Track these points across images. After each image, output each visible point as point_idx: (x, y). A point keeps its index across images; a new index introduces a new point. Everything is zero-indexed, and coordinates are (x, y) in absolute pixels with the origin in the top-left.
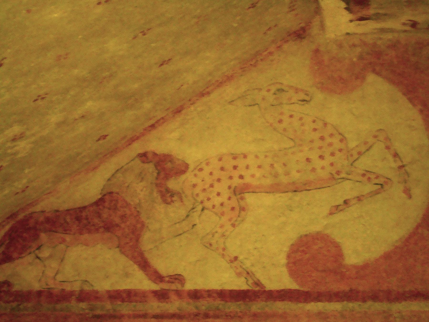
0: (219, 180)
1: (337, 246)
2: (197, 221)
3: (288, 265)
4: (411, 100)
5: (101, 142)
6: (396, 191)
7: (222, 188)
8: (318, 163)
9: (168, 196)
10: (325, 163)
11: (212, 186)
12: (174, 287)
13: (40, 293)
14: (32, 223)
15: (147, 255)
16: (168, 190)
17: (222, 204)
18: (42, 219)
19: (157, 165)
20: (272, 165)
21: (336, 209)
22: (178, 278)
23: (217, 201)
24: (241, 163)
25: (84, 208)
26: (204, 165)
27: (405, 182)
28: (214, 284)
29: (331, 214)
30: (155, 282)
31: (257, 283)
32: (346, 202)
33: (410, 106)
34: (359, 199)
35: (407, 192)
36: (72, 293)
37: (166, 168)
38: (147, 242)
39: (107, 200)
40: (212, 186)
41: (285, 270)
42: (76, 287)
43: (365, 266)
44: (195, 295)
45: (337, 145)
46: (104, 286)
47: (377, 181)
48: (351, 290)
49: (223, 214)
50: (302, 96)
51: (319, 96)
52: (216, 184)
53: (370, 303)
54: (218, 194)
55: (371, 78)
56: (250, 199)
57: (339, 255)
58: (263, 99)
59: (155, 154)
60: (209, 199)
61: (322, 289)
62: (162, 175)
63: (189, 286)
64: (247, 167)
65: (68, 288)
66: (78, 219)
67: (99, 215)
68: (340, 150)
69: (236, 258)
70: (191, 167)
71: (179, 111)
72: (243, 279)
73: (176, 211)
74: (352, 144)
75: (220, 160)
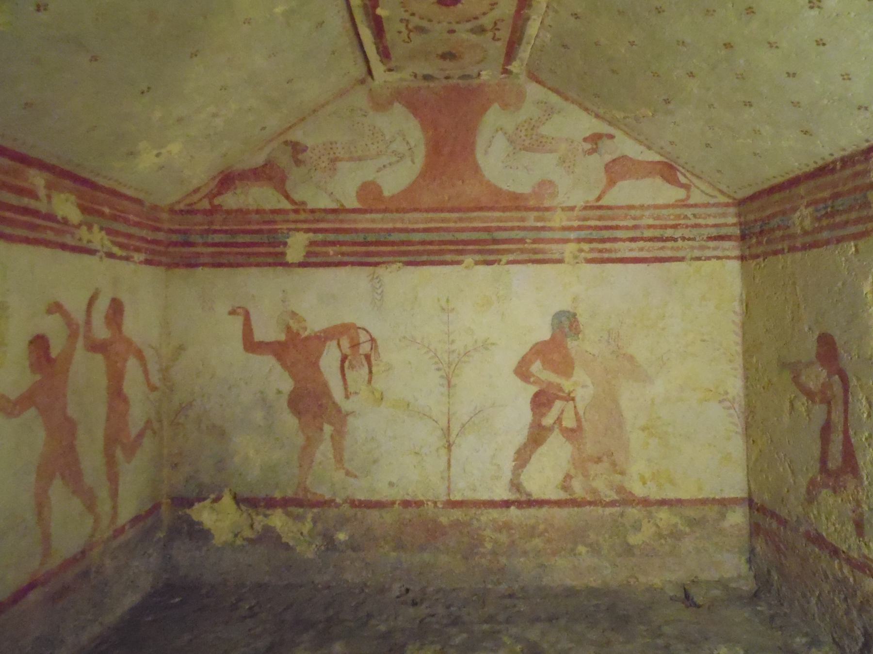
9: (298, 163)
10: (374, 147)
23: (323, 165)
24: (334, 146)
28: (322, 206)
31: (342, 205)
32: (384, 166)
34: (390, 164)
35: (413, 162)
37: (297, 149)
38: (289, 186)
39: (269, 164)
42: (255, 207)
43: (393, 196)
44: (313, 211)
46: (268, 207)
56: (339, 165)
57: (381, 192)
61: (374, 208)
63: (310, 206)
65: (251, 208)
66: (255, 174)
74: (387, 138)
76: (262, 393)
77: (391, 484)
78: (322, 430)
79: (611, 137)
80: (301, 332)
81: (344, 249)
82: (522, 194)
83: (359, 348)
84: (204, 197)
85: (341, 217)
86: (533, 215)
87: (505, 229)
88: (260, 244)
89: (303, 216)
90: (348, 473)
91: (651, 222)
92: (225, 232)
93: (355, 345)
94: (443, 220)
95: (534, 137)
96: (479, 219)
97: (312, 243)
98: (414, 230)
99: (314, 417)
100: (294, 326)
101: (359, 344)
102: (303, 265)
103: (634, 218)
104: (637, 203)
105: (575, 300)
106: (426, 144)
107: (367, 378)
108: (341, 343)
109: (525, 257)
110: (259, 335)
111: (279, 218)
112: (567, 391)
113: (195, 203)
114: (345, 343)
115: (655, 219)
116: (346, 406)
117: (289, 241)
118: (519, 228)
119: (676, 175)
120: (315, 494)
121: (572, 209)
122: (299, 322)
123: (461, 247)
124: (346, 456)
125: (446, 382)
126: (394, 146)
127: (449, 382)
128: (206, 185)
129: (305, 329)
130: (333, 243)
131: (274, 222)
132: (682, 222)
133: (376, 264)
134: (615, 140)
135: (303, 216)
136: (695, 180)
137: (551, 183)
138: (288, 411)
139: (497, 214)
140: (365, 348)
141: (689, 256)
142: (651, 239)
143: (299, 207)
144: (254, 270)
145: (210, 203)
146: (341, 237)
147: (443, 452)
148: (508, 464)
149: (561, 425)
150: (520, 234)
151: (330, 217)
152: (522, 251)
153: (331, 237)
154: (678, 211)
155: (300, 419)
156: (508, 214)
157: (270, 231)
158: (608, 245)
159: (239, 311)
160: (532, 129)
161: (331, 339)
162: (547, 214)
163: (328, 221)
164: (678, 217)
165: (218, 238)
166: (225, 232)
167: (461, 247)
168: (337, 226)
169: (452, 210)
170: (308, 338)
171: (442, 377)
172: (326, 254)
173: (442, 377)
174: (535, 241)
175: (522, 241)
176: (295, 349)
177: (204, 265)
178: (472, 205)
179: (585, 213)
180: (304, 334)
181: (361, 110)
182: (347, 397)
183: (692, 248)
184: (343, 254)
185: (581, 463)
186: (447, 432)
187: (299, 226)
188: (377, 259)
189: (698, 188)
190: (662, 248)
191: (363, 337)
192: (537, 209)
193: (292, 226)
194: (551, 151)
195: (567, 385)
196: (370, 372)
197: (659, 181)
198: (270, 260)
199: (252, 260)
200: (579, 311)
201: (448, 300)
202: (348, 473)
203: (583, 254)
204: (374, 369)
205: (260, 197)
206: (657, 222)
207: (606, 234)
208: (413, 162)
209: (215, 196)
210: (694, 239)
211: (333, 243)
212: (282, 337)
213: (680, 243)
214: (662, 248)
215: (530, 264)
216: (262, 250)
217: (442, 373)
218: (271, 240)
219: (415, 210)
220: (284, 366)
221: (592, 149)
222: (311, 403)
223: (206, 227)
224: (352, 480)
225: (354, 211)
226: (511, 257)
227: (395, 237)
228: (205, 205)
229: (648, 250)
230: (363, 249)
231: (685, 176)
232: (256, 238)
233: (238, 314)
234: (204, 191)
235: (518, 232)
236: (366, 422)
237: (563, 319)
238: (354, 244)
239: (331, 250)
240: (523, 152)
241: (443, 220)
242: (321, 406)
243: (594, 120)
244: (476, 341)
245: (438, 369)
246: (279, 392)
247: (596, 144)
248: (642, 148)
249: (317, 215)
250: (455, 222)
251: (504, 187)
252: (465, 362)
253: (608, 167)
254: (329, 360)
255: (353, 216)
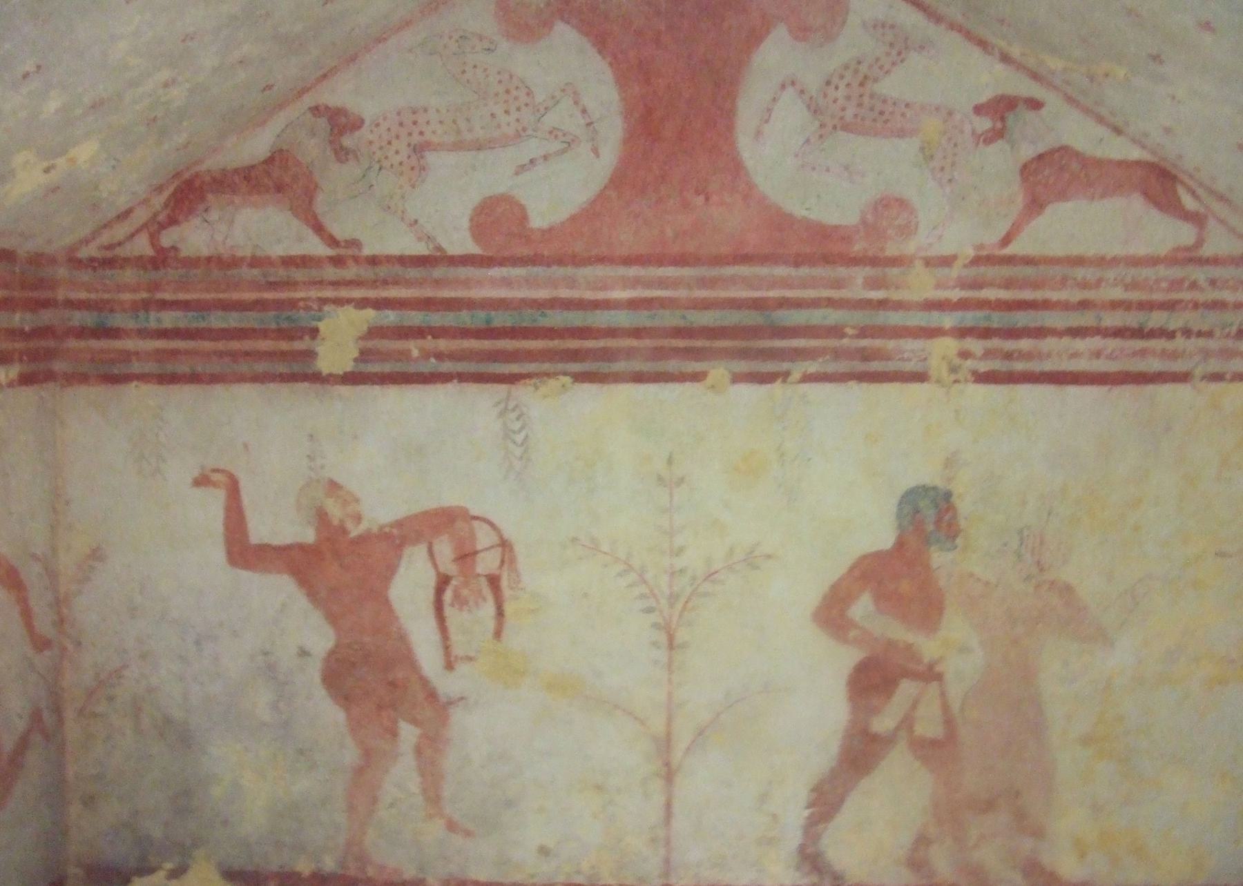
0: (398, 137)
1: (522, 208)
2: (374, 183)
3: (471, 229)
4: (600, 52)
5: (267, 92)
6: (584, 149)
7: (402, 145)
8: (503, 119)
9: (342, 154)
11: (389, 143)
12: (350, 252)
13: (209, 259)
14: (197, 183)
15: (319, 217)
16: (342, 148)
17: (401, 164)
18: (208, 179)
19: (331, 119)
20: (454, 122)
21: (521, 169)
22: (354, 243)
23: (396, 159)
25: (253, 167)
26: (381, 121)
27: (593, 139)
29: (517, 174)
30: (329, 246)
31: (439, 248)
32: (532, 161)
33: (599, 57)
34: (545, 158)
35: (596, 151)
36: (242, 259)
37: (340, 123)
38: (321, 205)
39: (278, 158)
40: (389, 143)
41: (467, 234)
42: (247, 252)
43: (551, 229)
44: (374, 261)
45: (524, 99)
47: (564, 139)
48: (536, 255)
49: (402, 174)
50: (486, 45)
51: (504, 45)
52: (395, 142)
53: (555, 268)
54: (397, 152)
55: (560, 27)
56: (431, 158)
57: (524, 218)
58: (445, 46)
59: (327, 108)
60: (386, 158)
61: (506, 254)
62: (336, 131)
63: (367, 251)
64: (428, 123)
65: (240, 254)
66: (247, 178)
67: (268, 174)
68: (527, 105)
69: (416, 221)
70: (367, 123)
71: (353, 59)
72: (423, 243)
73: (351, 170)
74: (540, 97)
75: (399, 114)
76: (266, 654)
77: (544, 851)
78: (394, 733)
79: (1035, 105)
80: (349, 525)
81: (443, 344)
82: (836, 228)
83: (474, 563)
84: (138, 231)
85: (439, 272)
86: (860, 274)
87: (798, 304)
88: (264, 334)
89: (351, 272)
90: (452, 826)
91: (1118, 294)
92: (185, 305)
93: (466, 557)
94: (662, 283)
95: (866, 100)
96: (743, 282)
97: (375, 332)
98: (596, 305)
99: (380, 707)
100: (335, 511)
101: (476, 553)
102: (352, 379)
103: (1084, 285)
104: (1091, 251)
105: (950, 462)
106: (627, 114)
107: (491, 625)
108: (436, 548)
109: (842, 366)
110: (261, 530)
111: (299, 275)
112: (926, 660)
113: (120, 244)
114: (445, 549)
115: (1127, 288)
116: (446, 685)
117: (322, 326)
118: (831, 303)
119: (1175, 192)
120: (382, 868)
121: (947, 261)
122: (345, 503)
123: (699, 343)
124: (447, 791)
125: (662, 638)
126: (550, 120)
127: (671, 639)
128: (145, 202)
129: (358, 518)
130: (419, 332)
131: (290, 284)
132: (1186, 296)
133: (512, 379)
134: (1044, 111)
135: (351, 272)
136: (1217, 207)
137: (902, 203)
138: (323, 692)
139: (781, 271)
140: (487, 563)
141: (1198, 372)
142: (1118, 333)
143: (344, 252)
144: (247, 392)
145: (153, 245)
146: (437, 319)
147: (657, 785)
148: (795, 815)
149: (910, 729)
150: (832, 317)
151: (413, 273)
152: (837, 354)
153: (415, 318)
154: (1176, 272)
155: (347, 710)
156: (804, 271)
157: (279, 305)
158: (1025, 344)
159: (216, 477)
160: (862, 84)
161: (417, 540)
162: (894, 272)
163: (409, 283)
164: (1176, 284)
165: (169, 319)
166: (185, 305)
167: (699, 343)
168: (428, 292)
169: (681, 260)
170: (364, 539)
171: (655, 626)
172: (404, 355)
173: (655, 626)
174: (864, 332)
175: (836, 331)
176: (337, 562)
177: (143, 378)
178: (725, 250)
179: (973, 272)
180: (355, 531)
181: (481, 38)
182: (449, 666)
183: (1206, 354)
184: (439, 356)
185: (951, 813)
186: (665, 744)
187: (344, 293)
188: (514, 368)
189: (1222, 222)
190: (1143, 353)
191: (484, 538)
192: (874, 261)
193: (329, 293)
194: (902, 133)
195: (929, 647)
196: (500, 613)
197: (1137, 204)
198: (282, 368)
199: (244, 367)
200: (958, 488)
201: (670, 461)
202: (452, 826)
203: (969, 363)
204: (509, 608)
205: (261, 229)
206: (1135, 296)
207: (1022, 319)
208: (596, 151)
209: (162, 227)
210: (1209, 334)
211: (419, 332)
212: (309, 536)
213: (1180, 342)
214: (1143, 353)
215: (853, 384)
216: (264, 345)
217: (654, 618)
218: (285, 325)
219: (601, 260)
220: (312, 595)
221: (993, 129)
222: (373, 679)
223: (145, 295)
224: (458, 840)
225: (466, 260)
226: (812, 367)
227: (556, 319)
228: (142, 246)
229: (1111, 357)
230: (486, 344)
231: (1193, 193)
232: (251, 320)
233: (215, 485)
234: (141, 216)
235: (829, 311)
236: (490, 725)
237: (922, 504)
238: (465, 333)
239: (414, 347)
240: (842, 135)
241: (662, 283)
242: (393, 684)
243: (999, 67)
244: (732, 550)
245: (649, 610)
246: (303, 653)
247: (1003, 119)
248: (1101, 131)
249: (383, 271)
250: (689, 287)
251: (799, 212)
252: (706, 594)
253: (1028, 171)
254: (411, 585)
255: (463, 272)
